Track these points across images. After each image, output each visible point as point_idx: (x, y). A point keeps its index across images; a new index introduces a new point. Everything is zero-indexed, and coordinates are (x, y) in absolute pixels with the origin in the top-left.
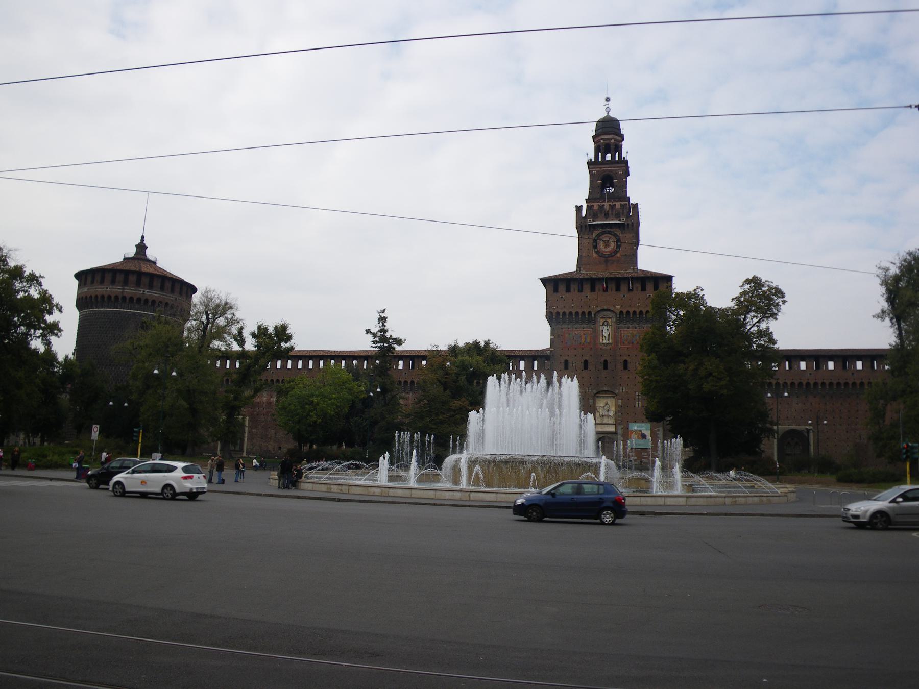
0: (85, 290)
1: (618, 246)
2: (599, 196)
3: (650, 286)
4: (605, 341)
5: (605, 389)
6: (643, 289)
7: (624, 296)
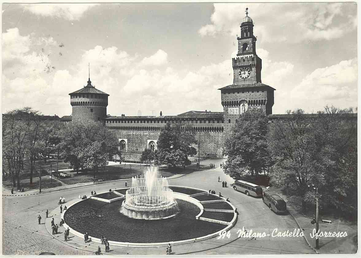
0: (72, 100)
2: (242, 53)
7: (250, 95)
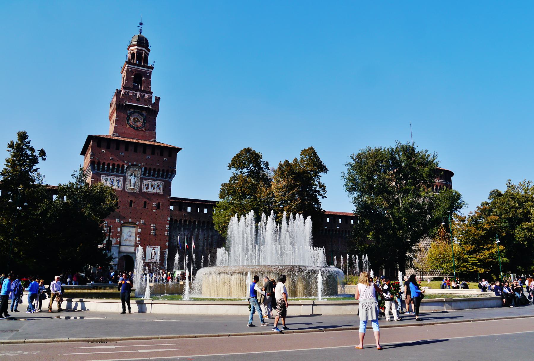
4: (132, 187)
5: (130, 220)
6: (162, 154)
7: (148, 157)
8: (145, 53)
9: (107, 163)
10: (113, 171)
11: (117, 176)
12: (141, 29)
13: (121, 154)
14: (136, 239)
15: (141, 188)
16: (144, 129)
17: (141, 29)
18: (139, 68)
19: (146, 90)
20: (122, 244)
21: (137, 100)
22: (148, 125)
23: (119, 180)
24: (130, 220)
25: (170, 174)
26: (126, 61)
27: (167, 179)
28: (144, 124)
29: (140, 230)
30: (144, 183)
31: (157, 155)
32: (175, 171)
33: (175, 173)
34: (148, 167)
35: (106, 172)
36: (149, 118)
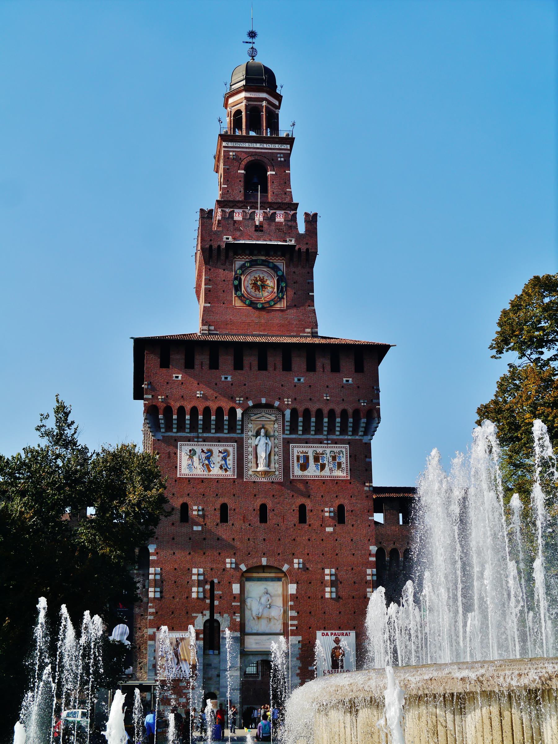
1: (280, 290)
2: (240, 198)
3: (347, 364)
4: (261, 468)
5: (264, 561)
6: (336, 368)
7: (299, 380)
8: (270, 107)
9: (188, 408)
10: (207, 428)
11: (219, 440)
12: (252, 48)
13: (223, 379)
14: (285, 612)
15: (286, 469)
16: (282, 305)
17: (252, 48)
18: (255, 145)
19: (279, 201)
20: (248, 630)
21: (256, 231)
22: (291, 293)
23: (226, 451)
24: (263, 559)
25: (364, 420)
26: (220, 135)
27: (357, 437)
28: (282, 291)
29: (295, 586)
30: (296, 454)
31: (324, 369)
32: (378, 411)
33: (379, 417)
34: (301, 409)
35: (190, 432)
36: (294, 272)
